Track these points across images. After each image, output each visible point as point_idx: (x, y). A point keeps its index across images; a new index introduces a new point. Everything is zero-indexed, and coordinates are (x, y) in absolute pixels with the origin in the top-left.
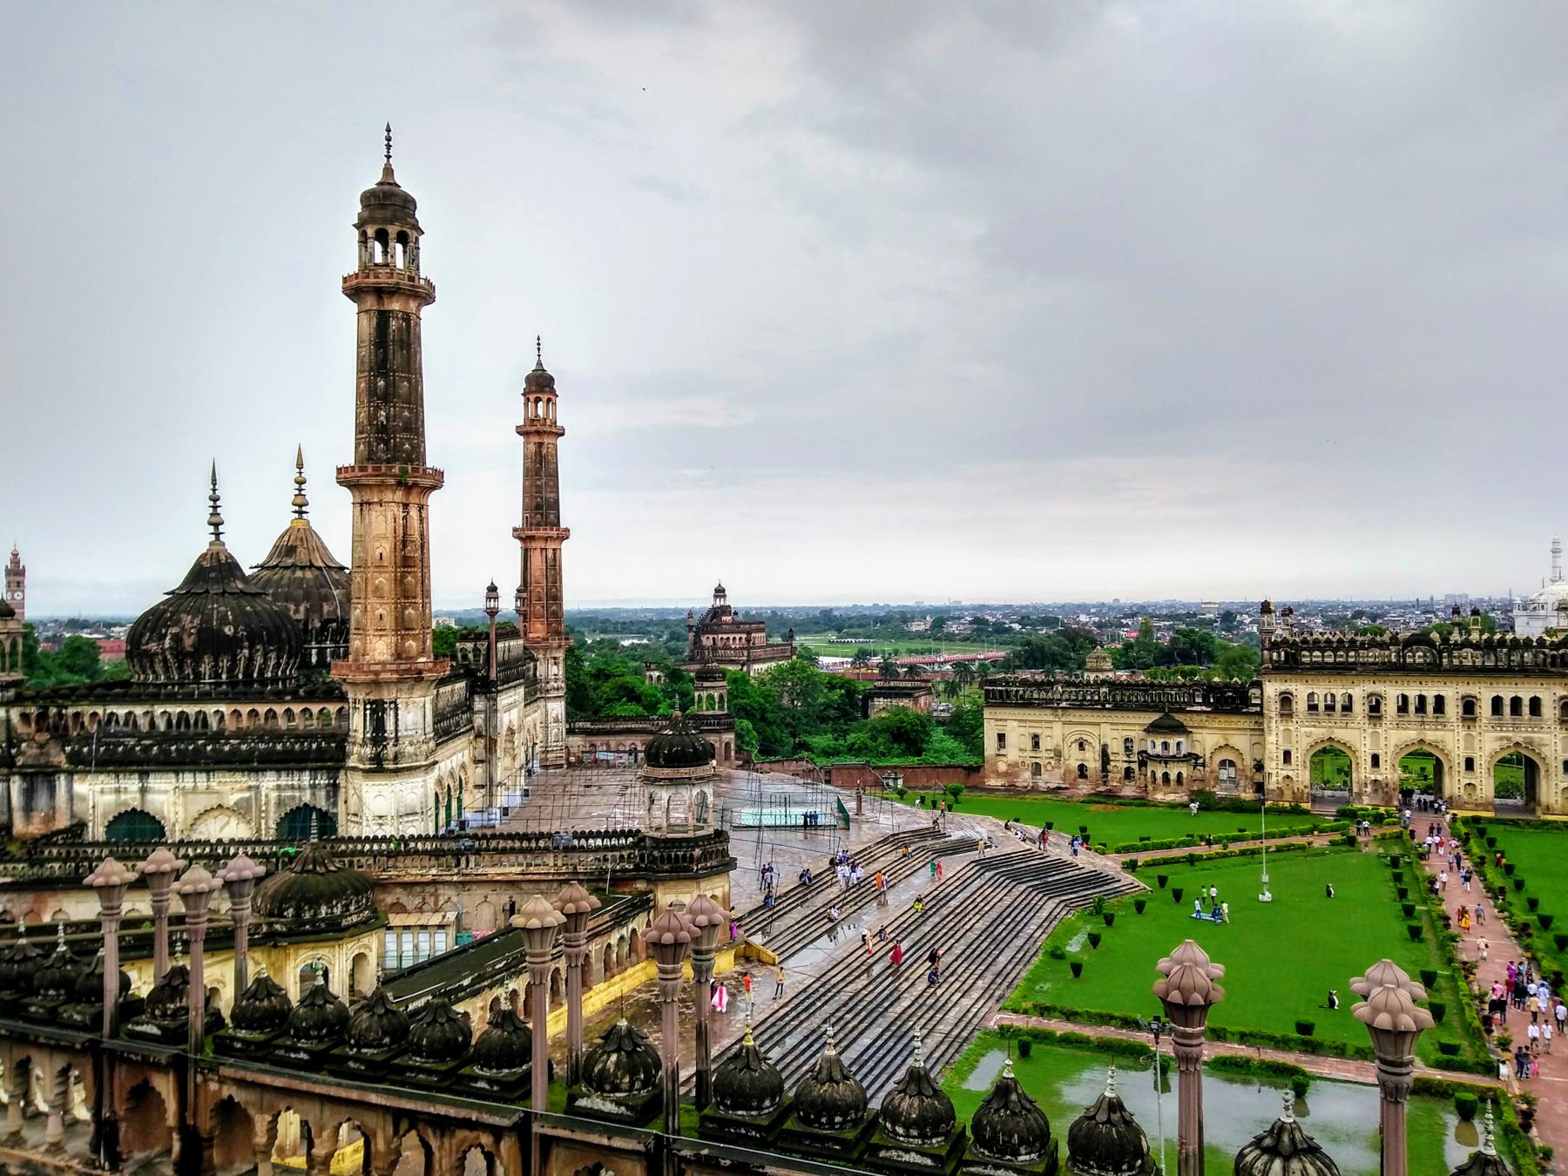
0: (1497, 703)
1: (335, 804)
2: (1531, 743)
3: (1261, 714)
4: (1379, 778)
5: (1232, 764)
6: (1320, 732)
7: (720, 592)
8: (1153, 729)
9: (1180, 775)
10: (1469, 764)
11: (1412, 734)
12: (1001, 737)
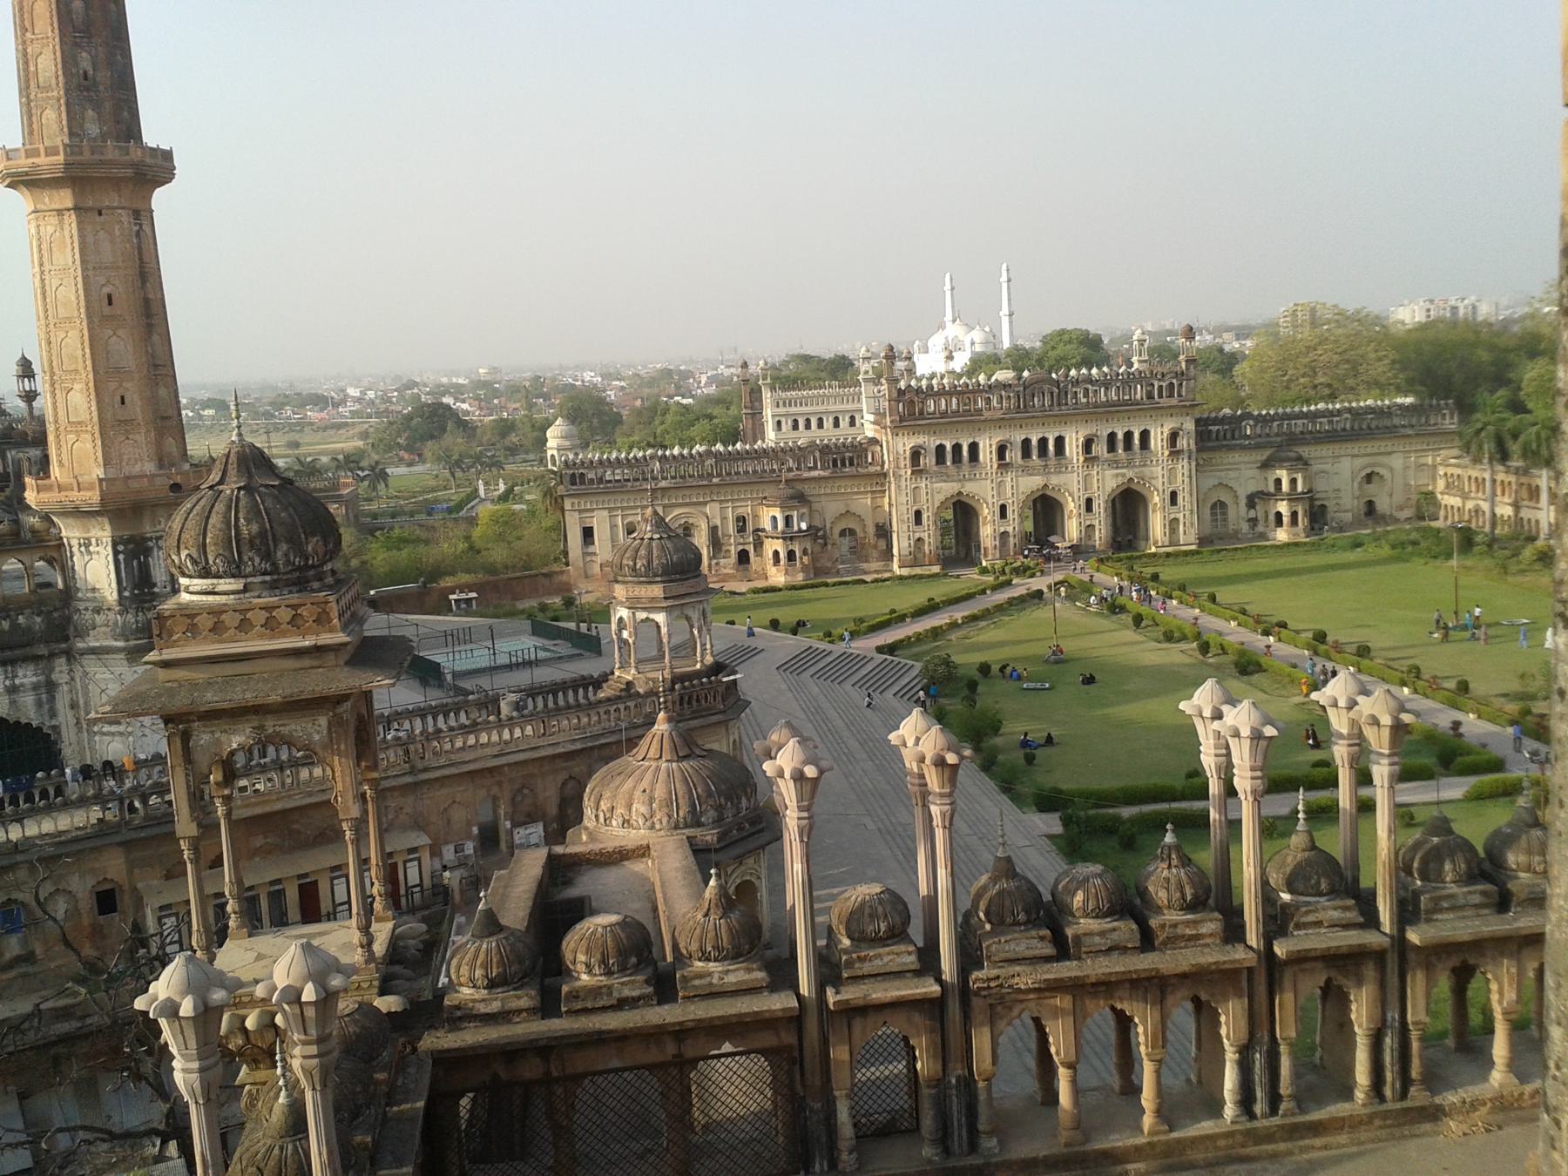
1: (53, 714)
5: (852, 532)
6: (948, 489)
12: (588, 533)
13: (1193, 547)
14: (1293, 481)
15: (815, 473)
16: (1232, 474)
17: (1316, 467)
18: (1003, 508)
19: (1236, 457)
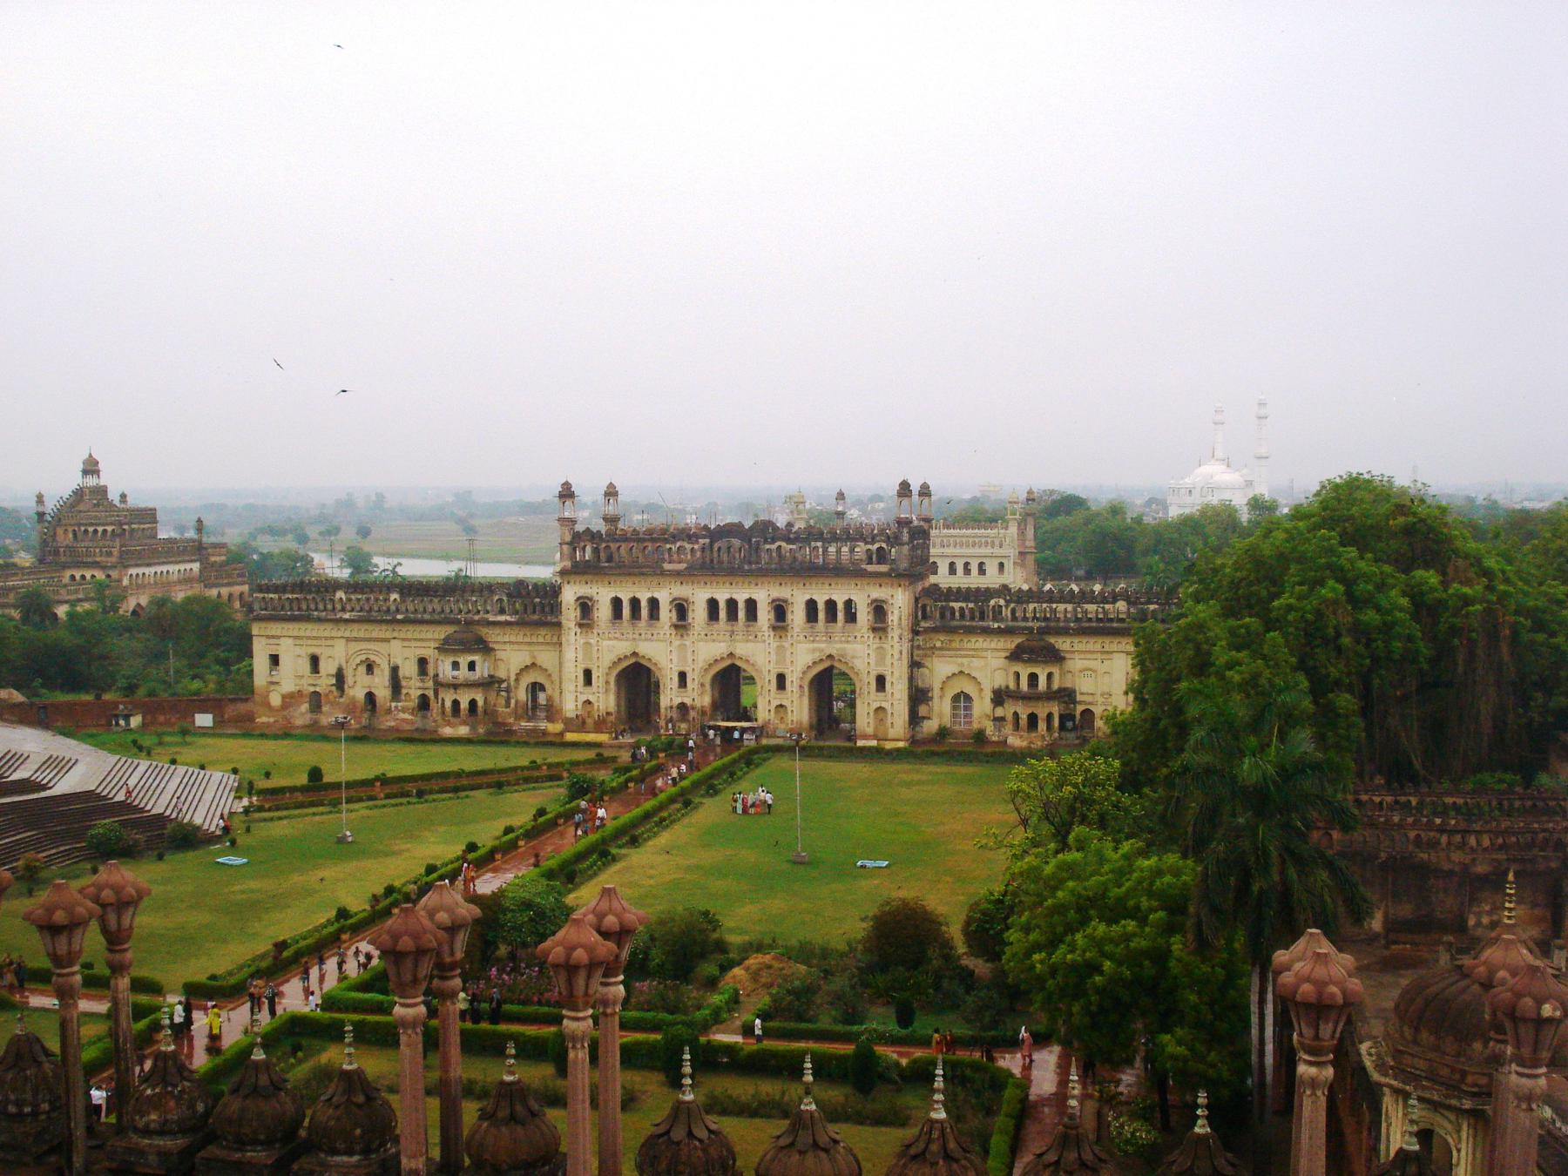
3: (559, 624)
4: (688, 701)
5: (542, 688)
7: (91, 468)
8: (445, 647)
9: (473, 703)
10: (781, 679)
12: (275, 660)
13: (901, 744)
14: (1033, 678)
15: (502, 618)
16: (976, 662)
17: (1076, 663)
18: (682, 676)
19: (980, 642)
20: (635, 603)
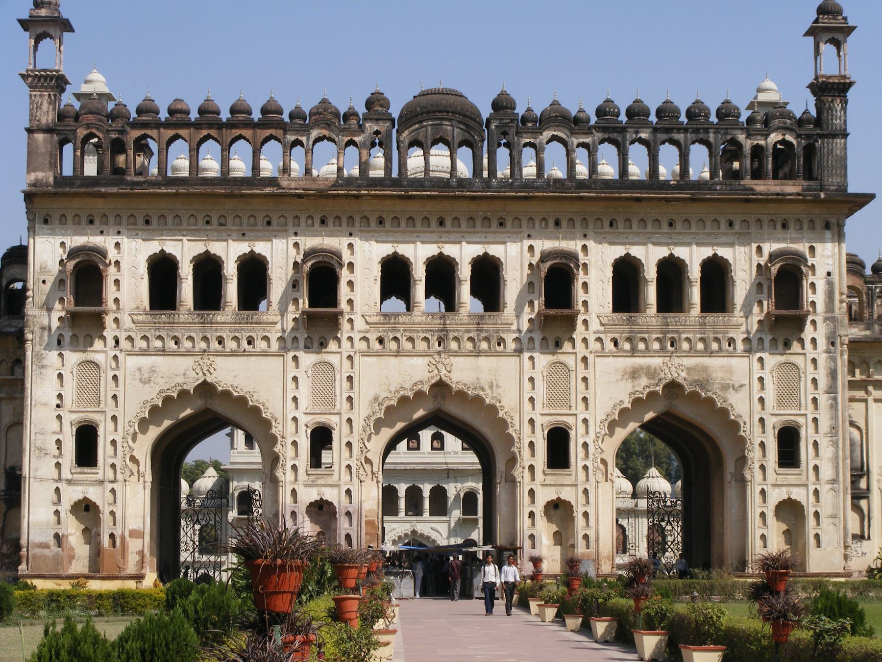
0: (626, 275)
2: (703, 384)
6: (178, 372)
11: (413, 372)
18: (321, 438)
20: (208, 270)
